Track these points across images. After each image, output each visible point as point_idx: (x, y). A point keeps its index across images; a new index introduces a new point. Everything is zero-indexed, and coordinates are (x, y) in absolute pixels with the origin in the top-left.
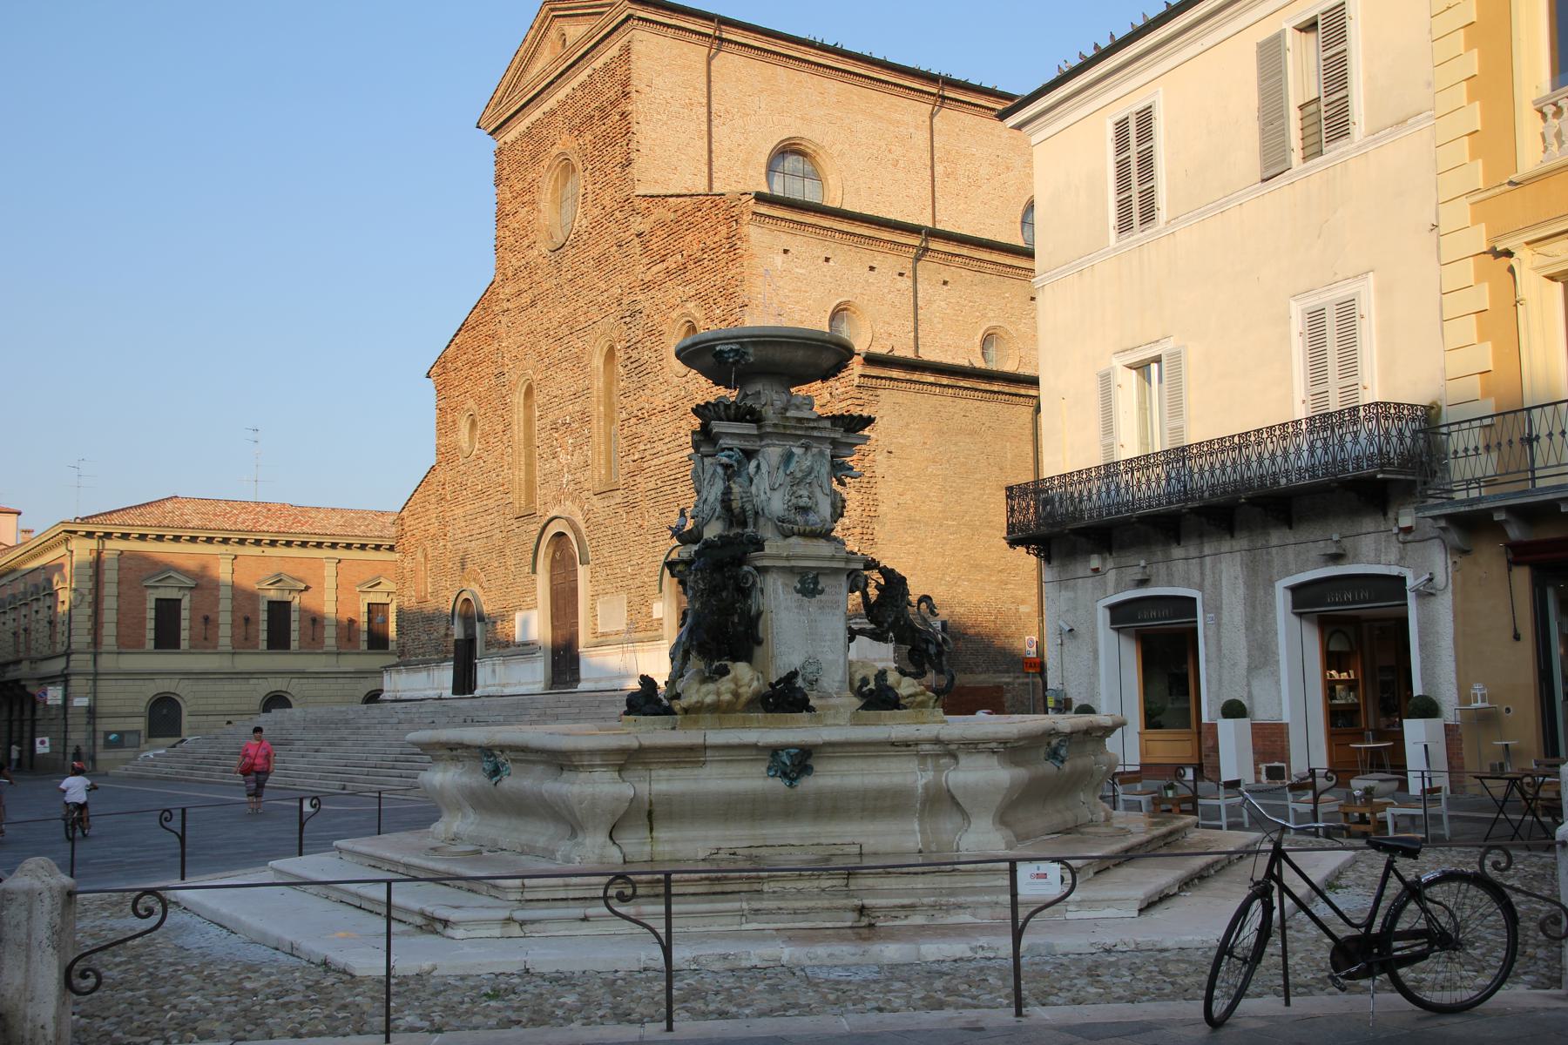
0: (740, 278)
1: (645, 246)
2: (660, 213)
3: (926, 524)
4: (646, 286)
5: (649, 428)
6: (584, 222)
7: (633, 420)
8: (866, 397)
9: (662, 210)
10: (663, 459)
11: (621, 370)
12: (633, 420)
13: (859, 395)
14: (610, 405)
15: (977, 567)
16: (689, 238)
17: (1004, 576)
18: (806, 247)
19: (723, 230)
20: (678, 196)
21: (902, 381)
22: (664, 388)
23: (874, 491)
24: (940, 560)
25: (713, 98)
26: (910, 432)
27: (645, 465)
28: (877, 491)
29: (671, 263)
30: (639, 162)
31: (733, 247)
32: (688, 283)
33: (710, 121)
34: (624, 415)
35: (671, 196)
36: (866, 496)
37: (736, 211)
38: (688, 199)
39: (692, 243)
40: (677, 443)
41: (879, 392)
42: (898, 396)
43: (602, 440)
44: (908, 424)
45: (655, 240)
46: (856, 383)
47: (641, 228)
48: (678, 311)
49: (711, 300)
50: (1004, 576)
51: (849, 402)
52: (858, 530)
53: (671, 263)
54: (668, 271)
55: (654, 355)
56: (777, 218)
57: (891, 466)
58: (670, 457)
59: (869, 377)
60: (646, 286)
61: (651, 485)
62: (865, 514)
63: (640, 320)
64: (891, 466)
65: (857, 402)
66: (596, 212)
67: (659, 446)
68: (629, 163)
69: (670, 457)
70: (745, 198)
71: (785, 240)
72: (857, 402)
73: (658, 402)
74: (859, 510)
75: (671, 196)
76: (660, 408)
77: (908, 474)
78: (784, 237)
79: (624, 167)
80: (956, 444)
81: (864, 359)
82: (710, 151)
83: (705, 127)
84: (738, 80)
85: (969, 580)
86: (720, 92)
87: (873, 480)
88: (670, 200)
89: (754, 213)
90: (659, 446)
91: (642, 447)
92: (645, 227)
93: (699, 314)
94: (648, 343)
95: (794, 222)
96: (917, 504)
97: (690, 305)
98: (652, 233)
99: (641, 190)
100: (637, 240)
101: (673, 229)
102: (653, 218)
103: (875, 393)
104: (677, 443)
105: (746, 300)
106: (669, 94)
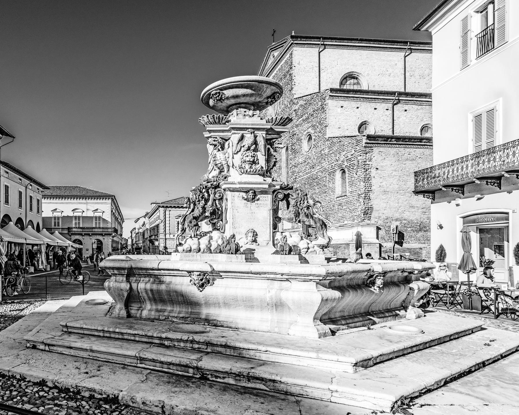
0: (325, 117)
1: (296, 113)
2: (301, 102)
3: (391, 192)
4: (297, 126)
5: (298, 169)
6: (280, 110)
7: (293, 167)
8: (368, 150)
9: (301, 101)
10: (302, 178)
11: (290, 152)
12: (293, 167)
13: (365, 150)
14: (287, 163)
15: (412, 207)
16: (309, 108)
17: (424, 210)
18: (350, 105)
19: (320, 103)
20: (306, 96)
21: (383, 144)
22: (302, 156)
23: (370, 182)
24: (397, 205)
25: (321, 64)
26: (385, 161)
27: (297, 180)
28: (371, 182)
29: (304, 117)
30: (295, 88)
31: (323, 108)
32: (309, 122)
33: (320, 71)
34: (291, 166)
35: (304, 96)
36: (367, 184)
37: (324, 96)
38: (309, 96)
39: (310, 110)
40: (306, 172)
41: (373, 148)
42: (381, 149)
43: (285, 174)
44: (385, 159)
45: (299, 111)
46: (364, 146)
47: (296, 108)
48: (306, 132)
49: (316, 127)
50: (424, 210)
51: (361, 152)
52: (364, 195)
53: (304, 117)
54: (303, 120)
55: (299, 147)
56: (339, 96)
57: (377, 173)
58: (303, 177)
59: (369, 143)
60: (297, 126)
61: (298, 186)
62: (366, 190)
63: (295, 137)
64: (377, 173)
65: (364, 152)
66: (283, 106)
67: (301, 174)
68: (292, 88)
69: (303, 177)
70: (326, 91)
71: (342, 103)
72: (364, 152)
73: (300, 160)
74: (364, 188)
75: (304, 96)
76: (301, 162)
77: (384, 176)
78: (341, 102)
79: (290, 91)
80: (405, 164)
81: (367, 137)
82: (320, 81)
83: (318, 74)
84: (330, 56)
85: (409, 211)
86: (323, 62)
87: (370, 178)
88: (304, 98)
89: (330, 96)
90: (301, 174)
91: (295, 175)
92: (297, 108)
93: (312, 132)
94: (298, 143)
95: (345, 97)
96: (388, 186)
97: (310, 129)
98: (299, 109)
99: (295, 97)
100: (294, 112)
101: (304, 107)
102: (299, 104)
103: (371, 149)
104: (306, 172)
105: (327, 124)
106: (305, 65)
